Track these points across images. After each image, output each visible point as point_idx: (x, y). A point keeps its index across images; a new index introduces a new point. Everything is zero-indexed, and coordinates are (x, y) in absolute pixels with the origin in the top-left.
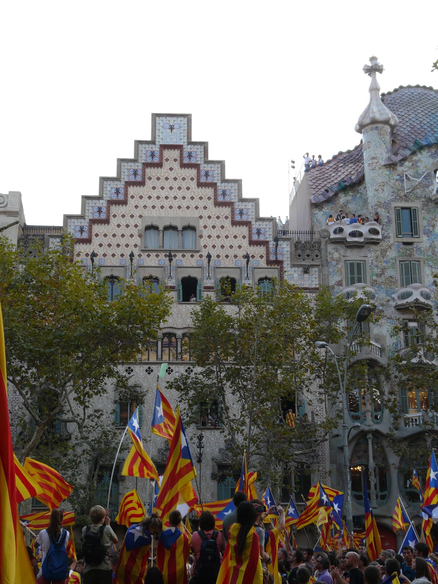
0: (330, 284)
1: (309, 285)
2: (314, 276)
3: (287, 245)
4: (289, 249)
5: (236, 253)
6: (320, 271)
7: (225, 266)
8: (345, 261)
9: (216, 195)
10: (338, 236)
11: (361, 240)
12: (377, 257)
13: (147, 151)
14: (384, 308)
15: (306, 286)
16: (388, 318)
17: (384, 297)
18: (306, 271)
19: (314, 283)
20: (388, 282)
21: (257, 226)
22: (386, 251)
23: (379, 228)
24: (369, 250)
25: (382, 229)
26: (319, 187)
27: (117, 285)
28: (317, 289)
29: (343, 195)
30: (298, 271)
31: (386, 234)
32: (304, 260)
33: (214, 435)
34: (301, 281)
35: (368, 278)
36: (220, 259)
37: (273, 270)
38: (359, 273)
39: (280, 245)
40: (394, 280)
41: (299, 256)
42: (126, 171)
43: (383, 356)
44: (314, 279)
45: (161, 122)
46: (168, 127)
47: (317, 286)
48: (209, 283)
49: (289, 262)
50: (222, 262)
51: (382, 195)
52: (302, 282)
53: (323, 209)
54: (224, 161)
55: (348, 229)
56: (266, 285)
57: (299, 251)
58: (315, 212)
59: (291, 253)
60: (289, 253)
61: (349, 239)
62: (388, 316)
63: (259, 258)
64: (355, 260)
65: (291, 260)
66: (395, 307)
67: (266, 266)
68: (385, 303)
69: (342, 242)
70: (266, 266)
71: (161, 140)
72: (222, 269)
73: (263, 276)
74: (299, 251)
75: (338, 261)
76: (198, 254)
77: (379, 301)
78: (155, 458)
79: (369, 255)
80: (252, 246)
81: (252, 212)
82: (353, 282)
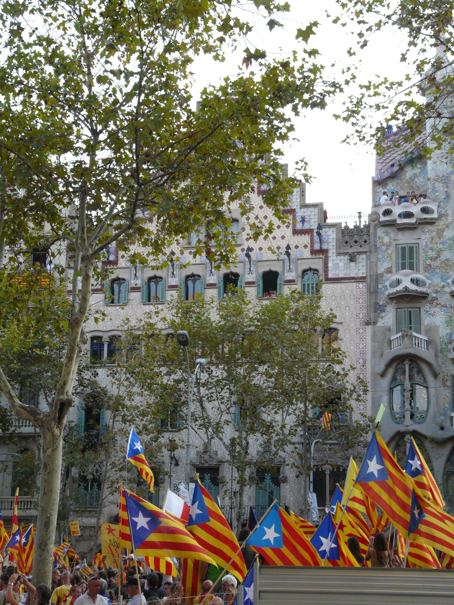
0: (379, 272)
1: (355, 274)
2: (361, 264)
3: (333, 232)
4: (334, 236)
5: (279, 244)
6: (368, 258)
7: (268, 259)
8: (397, 245)
10: (387, 218)
11: (413, 220)
12: (432, 239)
14: (438, 295)
15: (352, 275)
16: (443, 306)
17: (439, 282)
18: (352, 259)
19: (361, 271)
20: (443, 265)
21: (302, 214)
22: (442, 231)
23: (433, 206)
24: (423, 232)
25: (439, 206)
26: (387, 161)
27: (160, 285)
28: (364, 278)
29: (410, 169)
30: (344, 260)
31: (443, 212)
32: (351, 247)
34: (347, 270)
35: (421, 262)
36: (262, 252)
37: (318, 260)
38: (411, 257)
39: (326, 232)
40: (450, 263)
41: (346, 243)
43: (430, 349)
44: (361, 268)
47: (364, 275)
48: (250, 278)
49: (335, 251)
50: (265, 254)
51: (440, 168)
52: (348, 271)
53: (388, 187)
55: (397, 210)
56: (311, 277)
57: (347, 238)
58: (378, 190)
59: (336, 239)
60: (335, 240)
61: (399, 221)
62: (442, 304)
63: (303, 248)
64: (407, 244)
65: (336, 248)
66: (451, 293)
67: (310, 256)
68: (439, 289)
69: (391, 224)
70: (310, 256)
72: (264, 262)
73: (306, 267)
74: (347, 238)
75: (388, 246)
76: (240, 248)
77: (433, 288)
78: (193, 461)
79: (423, 237)
80: (296, 235)
81: (297, 199)
82: (403, 268)
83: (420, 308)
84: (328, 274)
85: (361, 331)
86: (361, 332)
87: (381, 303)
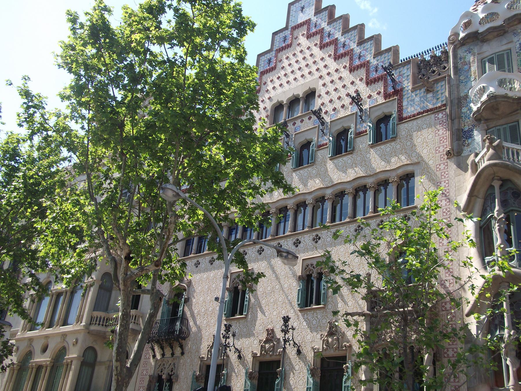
0: (462, 94)
2: (440, 92)
3: (407, 69)
9: (336, 50)
11: (499, 22)
13: (280, 38)
24: (514, 34)
33: (317, 317)
37: (391, 102)
42: (263, 62)
45: (295, 8)
46: (300, 9)
47: (444, 103)
54: (348, 14)
61: (482, 29)
64: (495, 53)
70: (384, 101)
71: (293, 23)
72: (337, 121)
83: (518, 121)
84: (402, 114)
85: (442, 167)
86: (442, 168)
87: (466, 128)
